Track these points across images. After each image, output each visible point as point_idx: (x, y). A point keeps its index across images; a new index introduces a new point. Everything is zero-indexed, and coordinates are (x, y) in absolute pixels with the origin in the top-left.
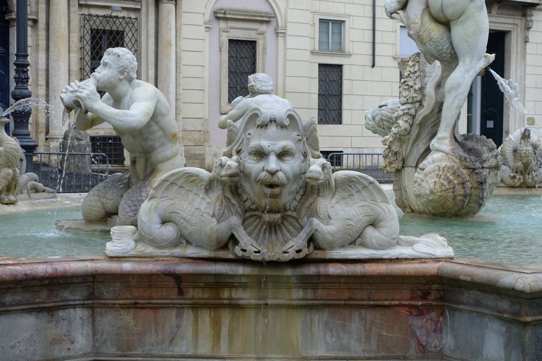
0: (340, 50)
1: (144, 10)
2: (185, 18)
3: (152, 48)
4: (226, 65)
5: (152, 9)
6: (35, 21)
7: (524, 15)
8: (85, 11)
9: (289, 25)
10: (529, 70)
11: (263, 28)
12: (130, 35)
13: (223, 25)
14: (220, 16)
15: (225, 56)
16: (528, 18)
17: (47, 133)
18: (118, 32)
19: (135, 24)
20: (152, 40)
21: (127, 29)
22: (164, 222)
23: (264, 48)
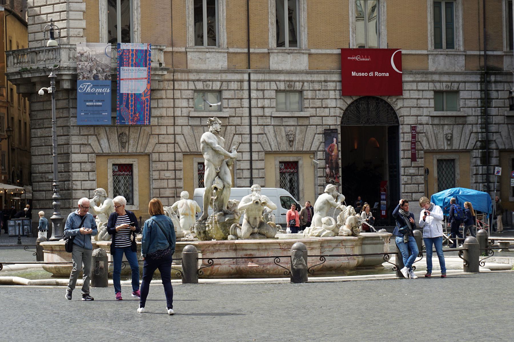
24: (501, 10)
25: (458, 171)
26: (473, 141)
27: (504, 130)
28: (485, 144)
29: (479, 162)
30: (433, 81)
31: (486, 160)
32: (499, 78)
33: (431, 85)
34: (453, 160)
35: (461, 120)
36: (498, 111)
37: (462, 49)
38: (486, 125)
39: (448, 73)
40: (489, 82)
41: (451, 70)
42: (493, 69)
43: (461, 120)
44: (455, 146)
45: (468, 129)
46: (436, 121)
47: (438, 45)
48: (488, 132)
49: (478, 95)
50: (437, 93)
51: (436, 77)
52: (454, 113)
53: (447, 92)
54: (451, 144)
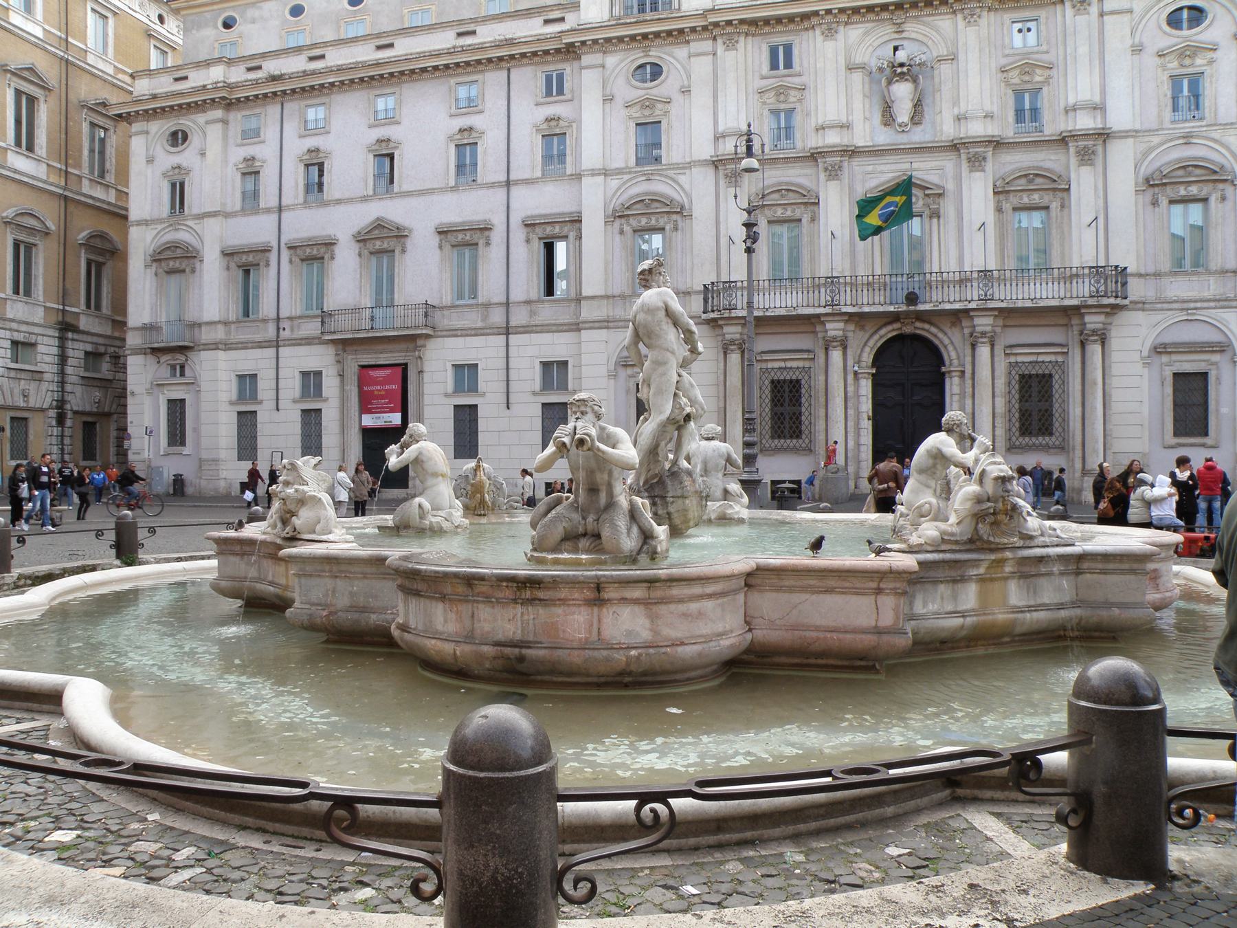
2: (1115, 357)
3: (1078, 387)
6: (963, 372)
8: (1013, 359)
11: (1216, 358)
12: (1057, 377)
13: (1165, 358)
15: (1169, 390)
18: (1044, 375)
19: (1061, 366)
20: (1078, 381)
21: (1053, 372)
23: (1218, 379)
24: (79, 266)
25: (31, 432)
26: (49, 400)
27: (79, 390)
28: (61, 404)
29: (54, 423)
30: (10, 330)
31: (61, 420)
32: (76, 336)
33: (8, 332)
34: (26, 419)
35: (37, 376)
36: (74, 369)
37: (41, 299)
38: (62, 383)
39: (27, 323)
40: (67, 339)
41: (30, 320)
42: (73, 326)
43: (37, 376)
44: (31, 404)
45: (45, 386)
46: (13, 374)
47: (16, 291)
48: (63, 391)
49: (55, 351)
50: (15, 343)
51: (14, 326)
52: (33, 368)
53: (25, 344)
54: (27, 402)
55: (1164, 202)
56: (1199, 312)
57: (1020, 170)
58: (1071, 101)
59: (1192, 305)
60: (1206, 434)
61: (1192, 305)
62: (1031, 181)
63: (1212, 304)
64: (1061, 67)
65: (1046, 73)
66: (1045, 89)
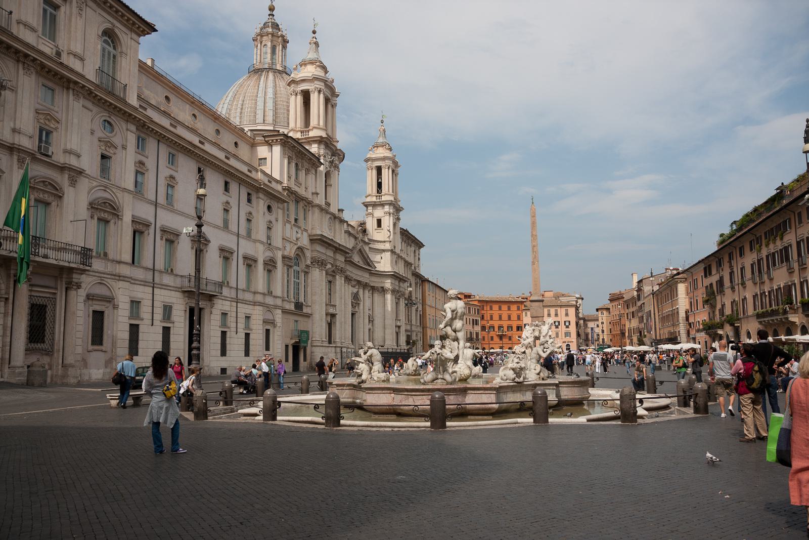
0: (138, 317)
1: (59, 293)
4: (91, 324)
5: (64, 293)
6: (7, 299)
7: (210, 300)
9: (120, 303)
10: (212, 328)
11: (108, 304)
13: (90, 302)
14: (90, 297)
15: (91, 320)
16: (212, 302)
17: (9, 363)
18: (43, 305)
22: (505, 376)
55: (96, 218)
56: (106, 280)
57: (43, 178)
58: (68, 147)
59: (103, 275)
60: (101, 344)
61: (103, 275)
62: (46, 186)
63: (109, 276)
64: (64, 125)
65: (57, 125)
66: (54, 133)
